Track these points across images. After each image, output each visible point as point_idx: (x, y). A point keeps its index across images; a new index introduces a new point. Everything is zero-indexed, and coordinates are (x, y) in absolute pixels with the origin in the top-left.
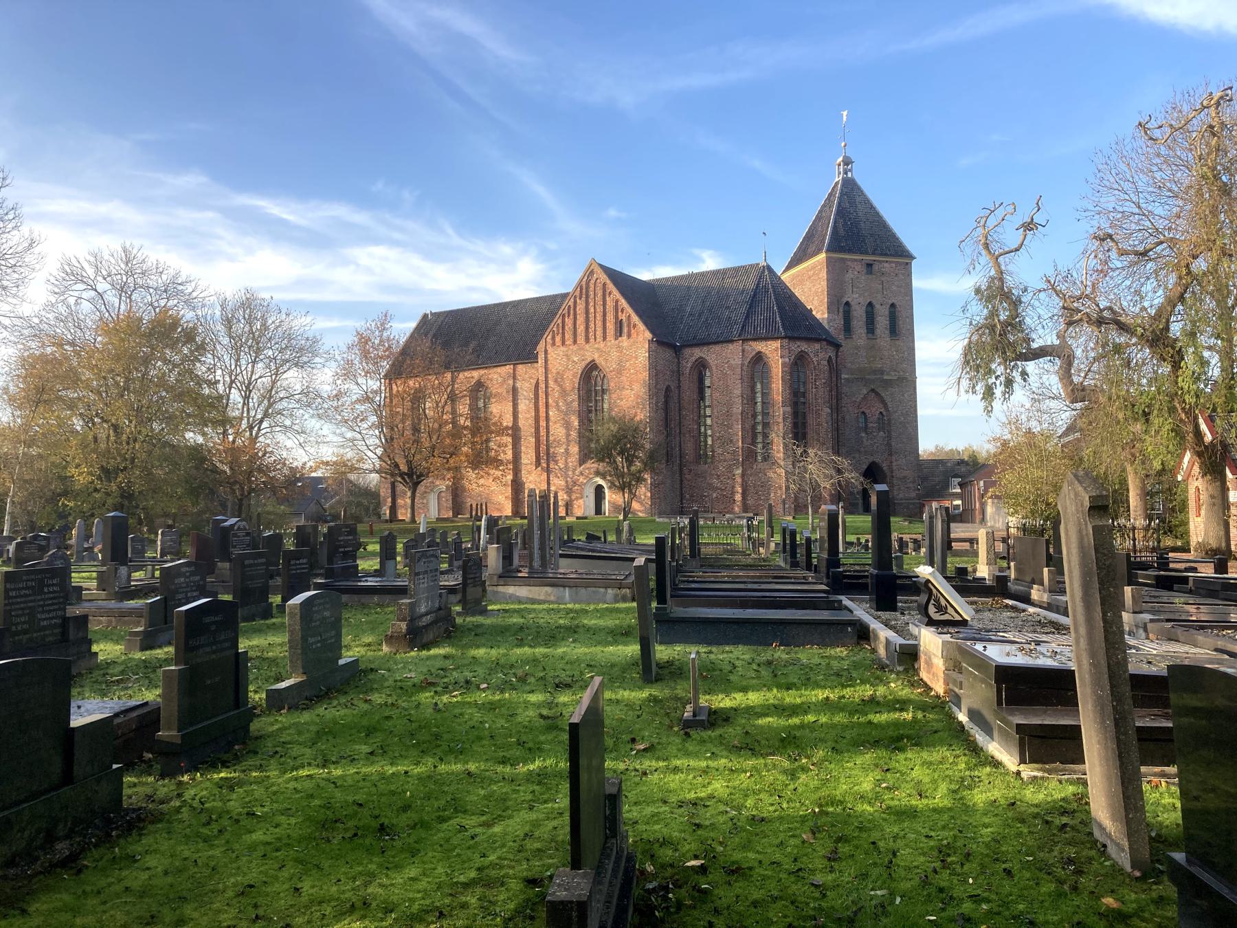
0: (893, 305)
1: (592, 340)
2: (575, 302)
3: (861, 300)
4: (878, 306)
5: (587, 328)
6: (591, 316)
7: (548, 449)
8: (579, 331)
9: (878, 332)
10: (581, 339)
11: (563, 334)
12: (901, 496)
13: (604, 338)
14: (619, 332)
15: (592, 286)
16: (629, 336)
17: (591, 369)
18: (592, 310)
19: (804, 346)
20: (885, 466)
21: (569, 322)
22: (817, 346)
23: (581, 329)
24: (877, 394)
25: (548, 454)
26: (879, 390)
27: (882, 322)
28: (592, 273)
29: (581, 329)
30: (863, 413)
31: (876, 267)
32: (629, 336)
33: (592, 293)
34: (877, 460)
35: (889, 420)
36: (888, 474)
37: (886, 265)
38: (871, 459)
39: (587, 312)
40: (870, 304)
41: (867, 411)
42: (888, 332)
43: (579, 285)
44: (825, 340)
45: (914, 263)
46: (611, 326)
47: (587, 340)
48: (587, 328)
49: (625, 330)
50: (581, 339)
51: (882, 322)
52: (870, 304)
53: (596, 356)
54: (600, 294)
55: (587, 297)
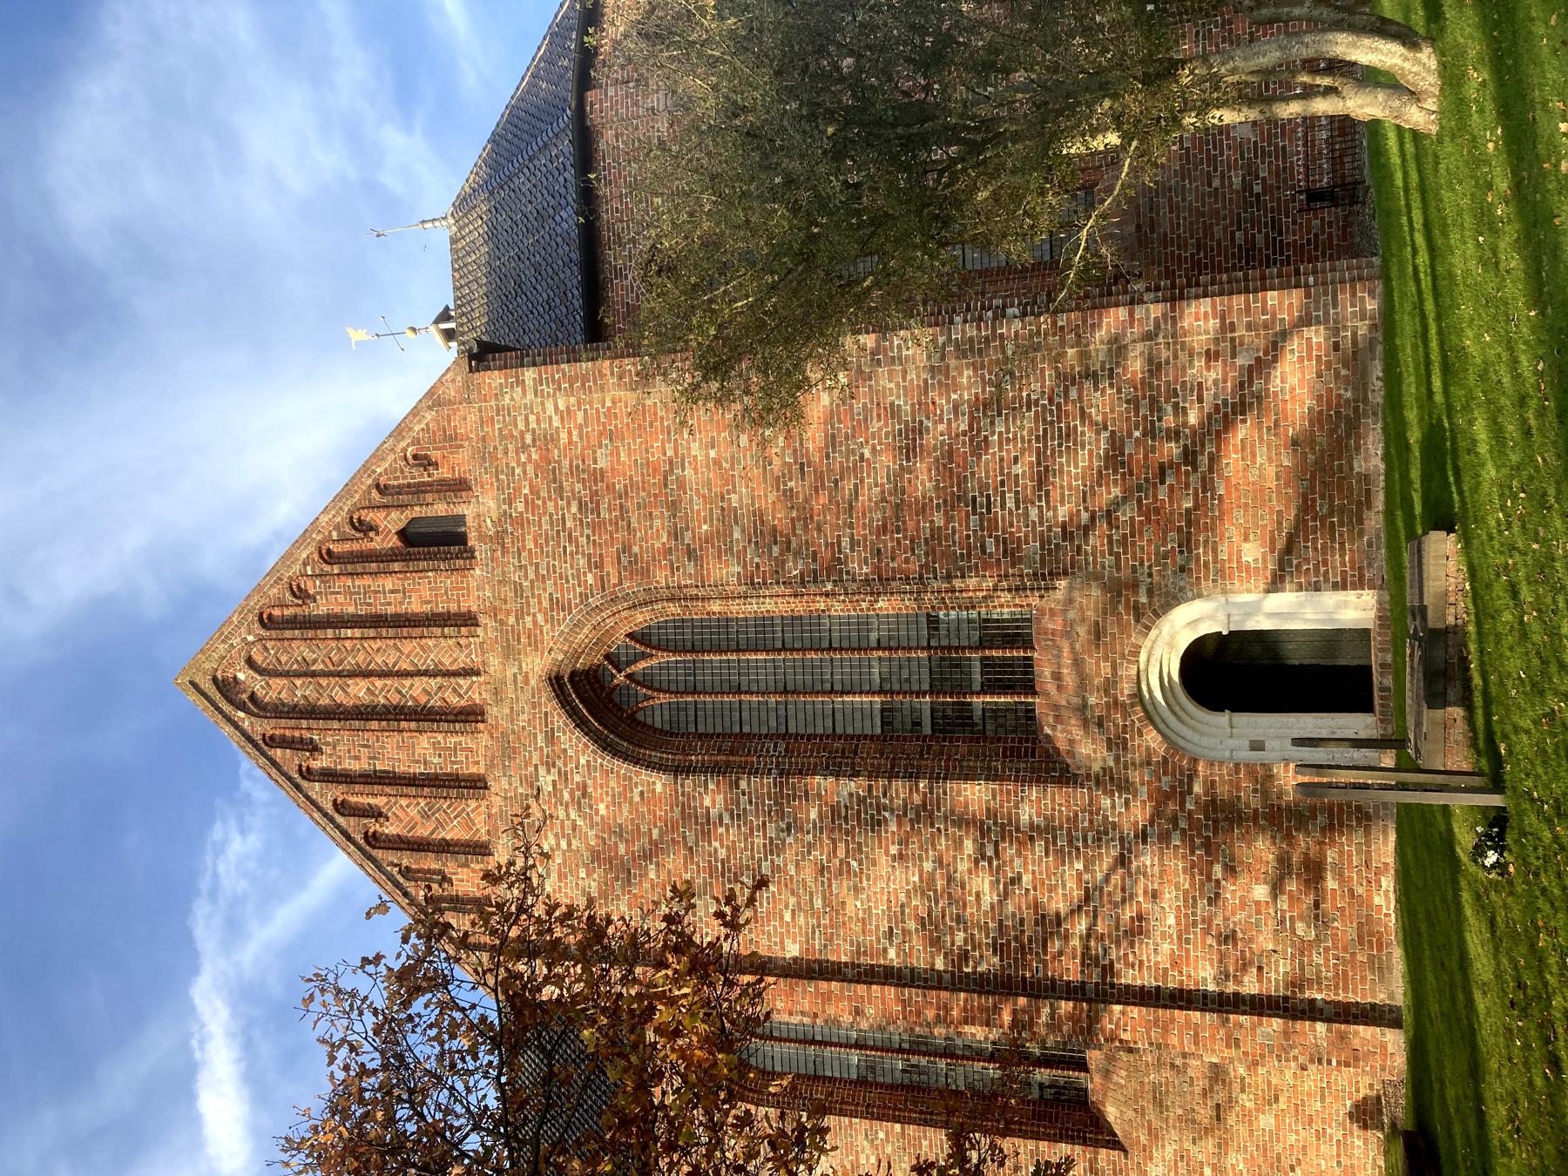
1: (471, 692)
2: (329, 776)
5: (424, 716)
6: (385, 692)
7: (980, 985)
8: (438, 764)
10: (466, 752)
11: (446, 848)
13: (467, 620)
14: (436, 543)
15: (274, 690)
16: (459, 486)
17: (599, 701)
18: (359, 691)
21: (405, 815)
23: (423, 751)
25: (1000, 986)
28: (227, 687)
29: (423, 751)
32: (459, 486)
33: (303, 691)
39: (362, 714)
43: (263, 746)
46: (422, 590)
47: (470, 716)
48: (424, 716)
49: (440, 509)
50: (466, 752)
53: (537, 665)
54: (303, 650)
55: (311, 712)
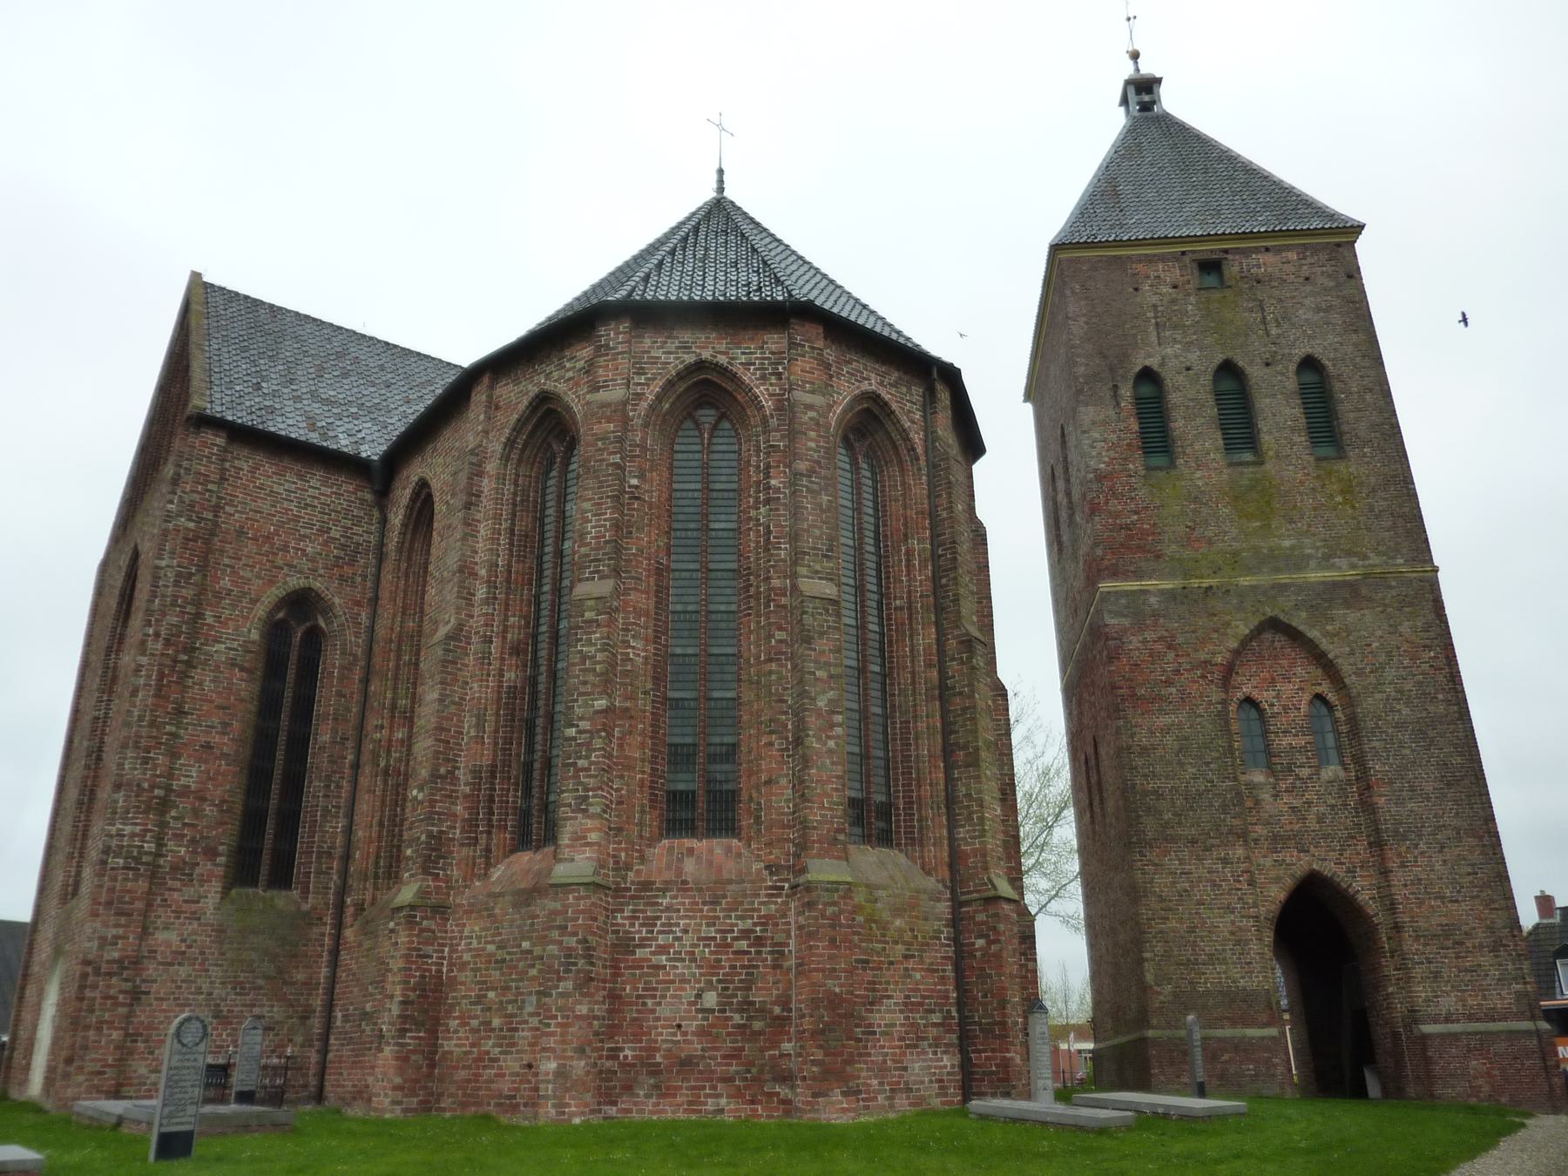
0: (1309, 364)
3: (1194, 356)
4: (1255, 372)
9: (1267, 439)
12: (1448, 1003)
19: (709, 346)
20: (1363, 889)
22: (774, 341)
24: (1294, 635)
26: (1299, 621)
27: (1279, 412)
30: (1249, 701)
31: (1232, 269)
34: (1328, 868)
35: (1353, 720)
36: (1380, 918)
37: (1269, 258)
38: (1301, 864)
40: (1228, 370)
41: (1265, 696)
42: (1301, 439)
44: (806, 312)
45: (1360, 246)
51: (1279, 412)
52: (1228, 370)
